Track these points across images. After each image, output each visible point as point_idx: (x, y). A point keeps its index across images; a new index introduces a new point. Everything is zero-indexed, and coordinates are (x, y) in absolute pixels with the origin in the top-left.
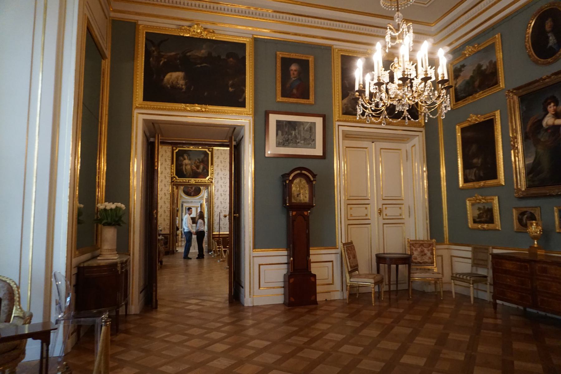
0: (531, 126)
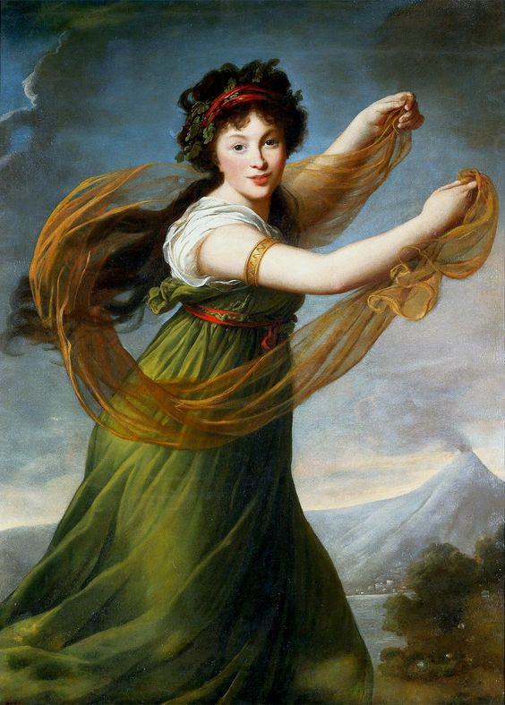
0: (70, 243)
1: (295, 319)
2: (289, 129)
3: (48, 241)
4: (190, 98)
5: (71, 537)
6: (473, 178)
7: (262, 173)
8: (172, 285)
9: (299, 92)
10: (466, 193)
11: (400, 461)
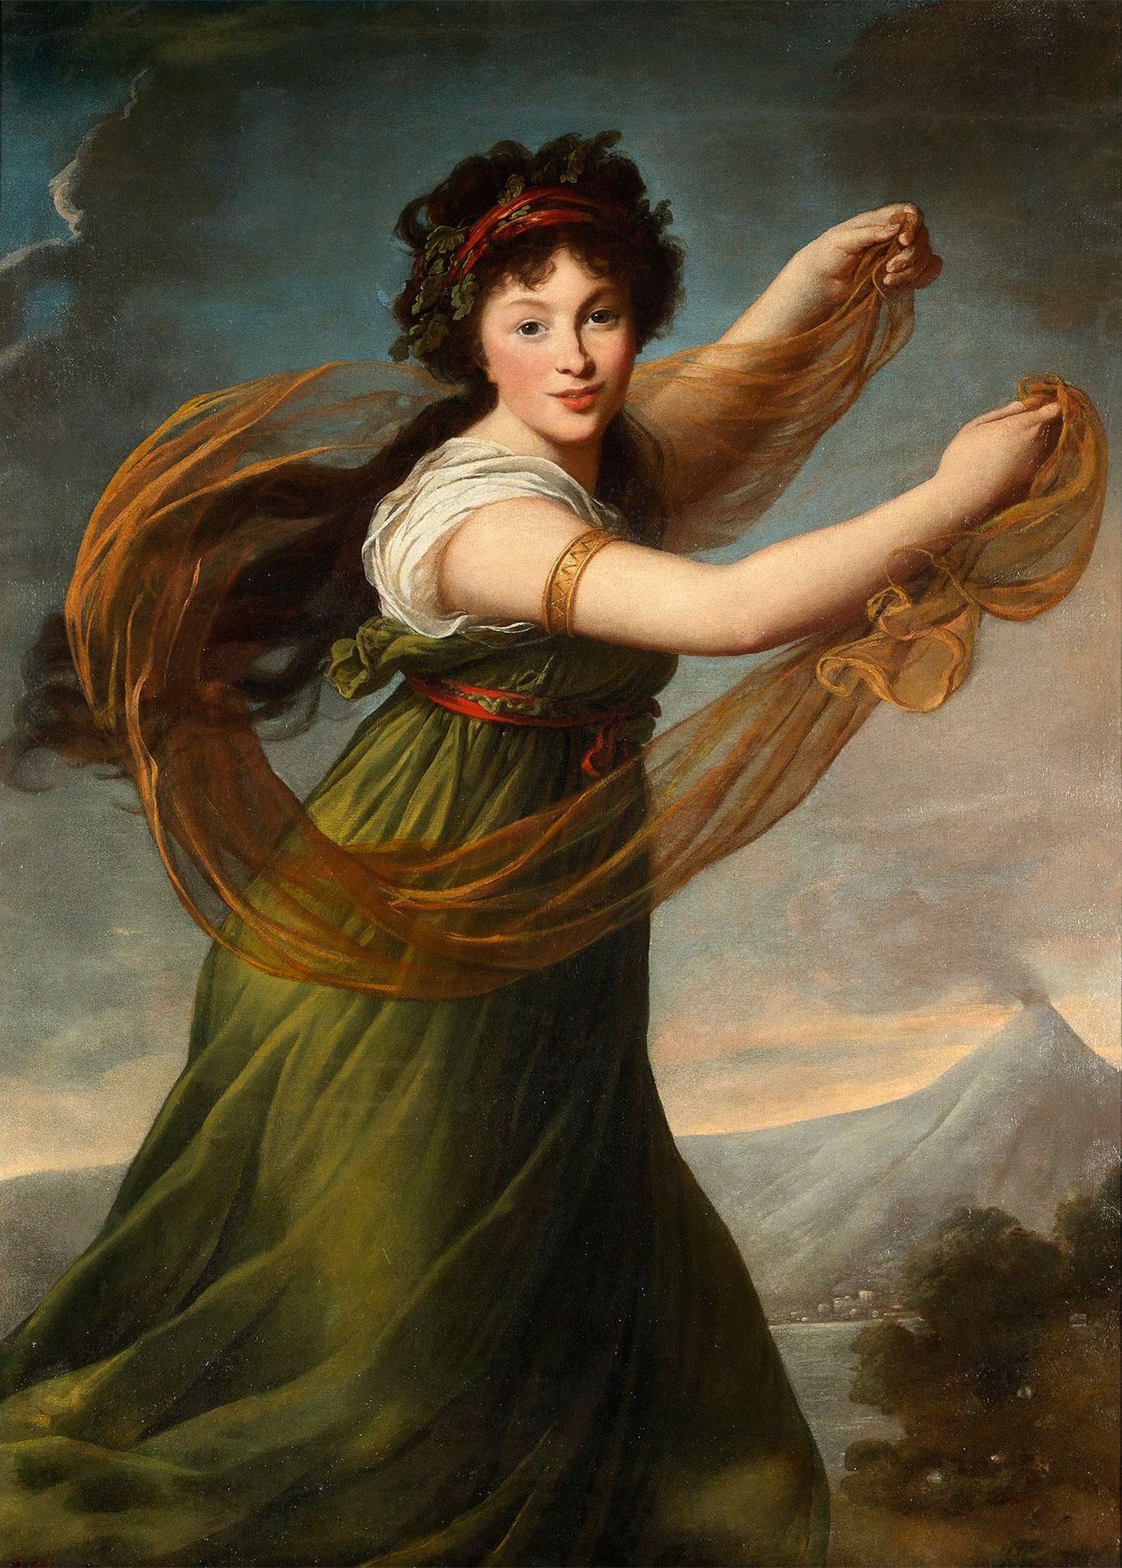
1: (656, 710)
2: (642, 289)
3: (107, 536)
4: (422, 218)
5: (156, 1195)
6: (1051, 396)
7: (581, 385)
8: (383, 634)
9: (664, 205)
10: (1034, 430)
11: (888, 1025)
